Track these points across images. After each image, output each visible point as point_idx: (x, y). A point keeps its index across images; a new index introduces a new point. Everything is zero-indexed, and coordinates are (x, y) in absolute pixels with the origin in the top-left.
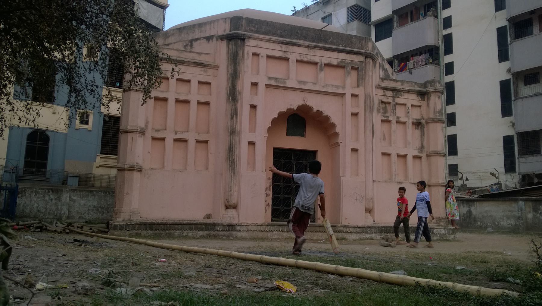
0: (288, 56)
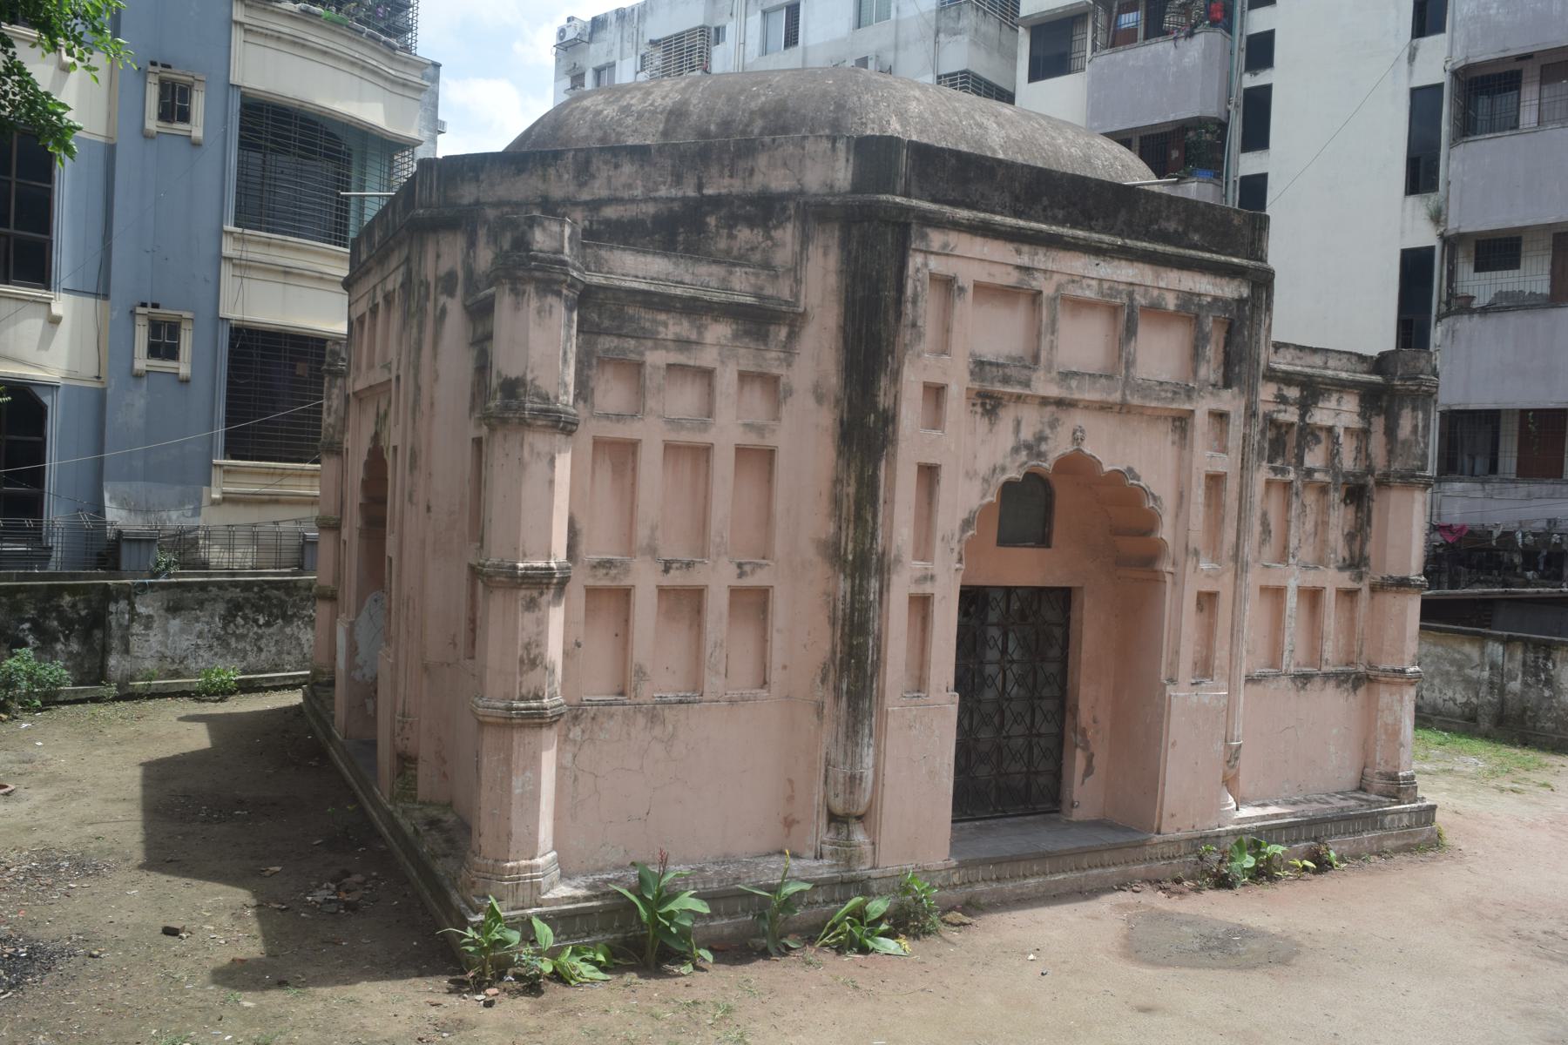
0: (1038, 282)
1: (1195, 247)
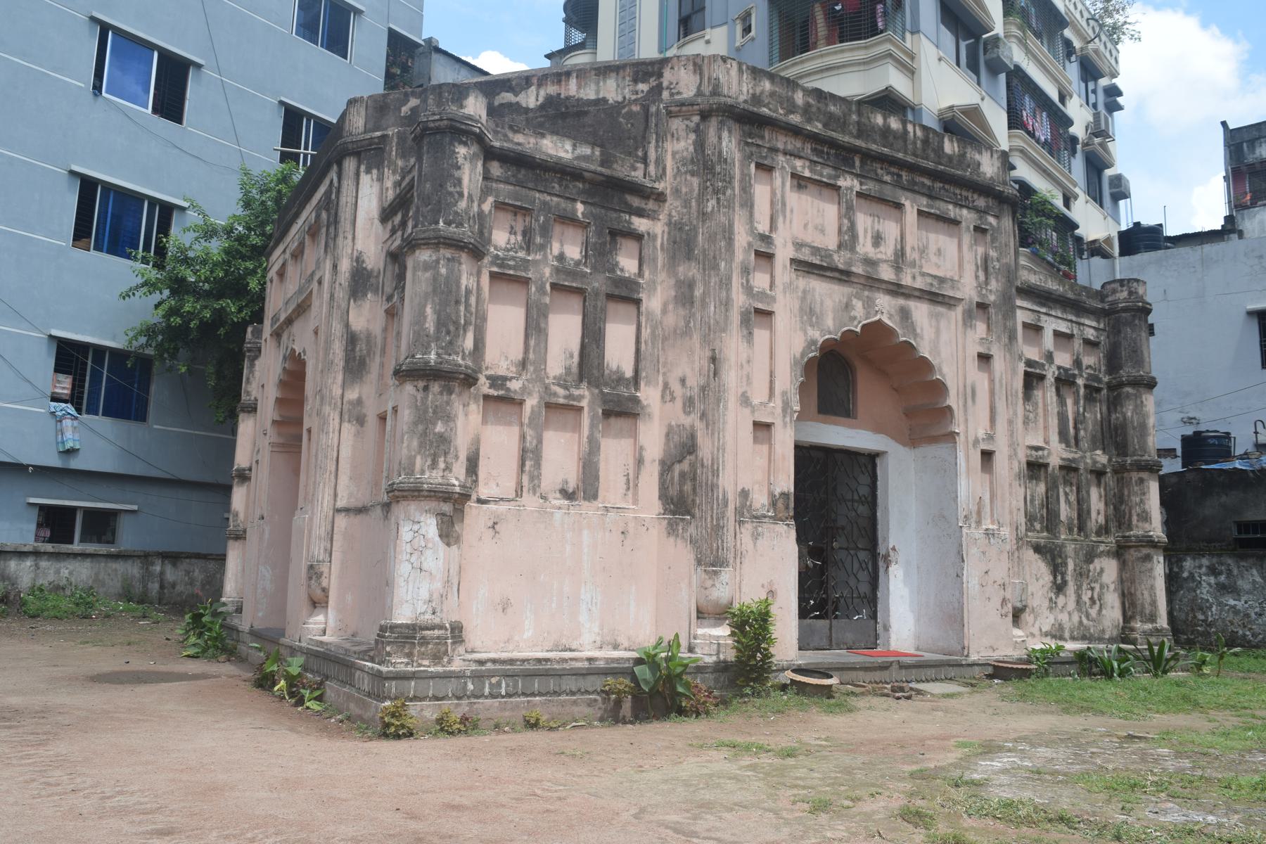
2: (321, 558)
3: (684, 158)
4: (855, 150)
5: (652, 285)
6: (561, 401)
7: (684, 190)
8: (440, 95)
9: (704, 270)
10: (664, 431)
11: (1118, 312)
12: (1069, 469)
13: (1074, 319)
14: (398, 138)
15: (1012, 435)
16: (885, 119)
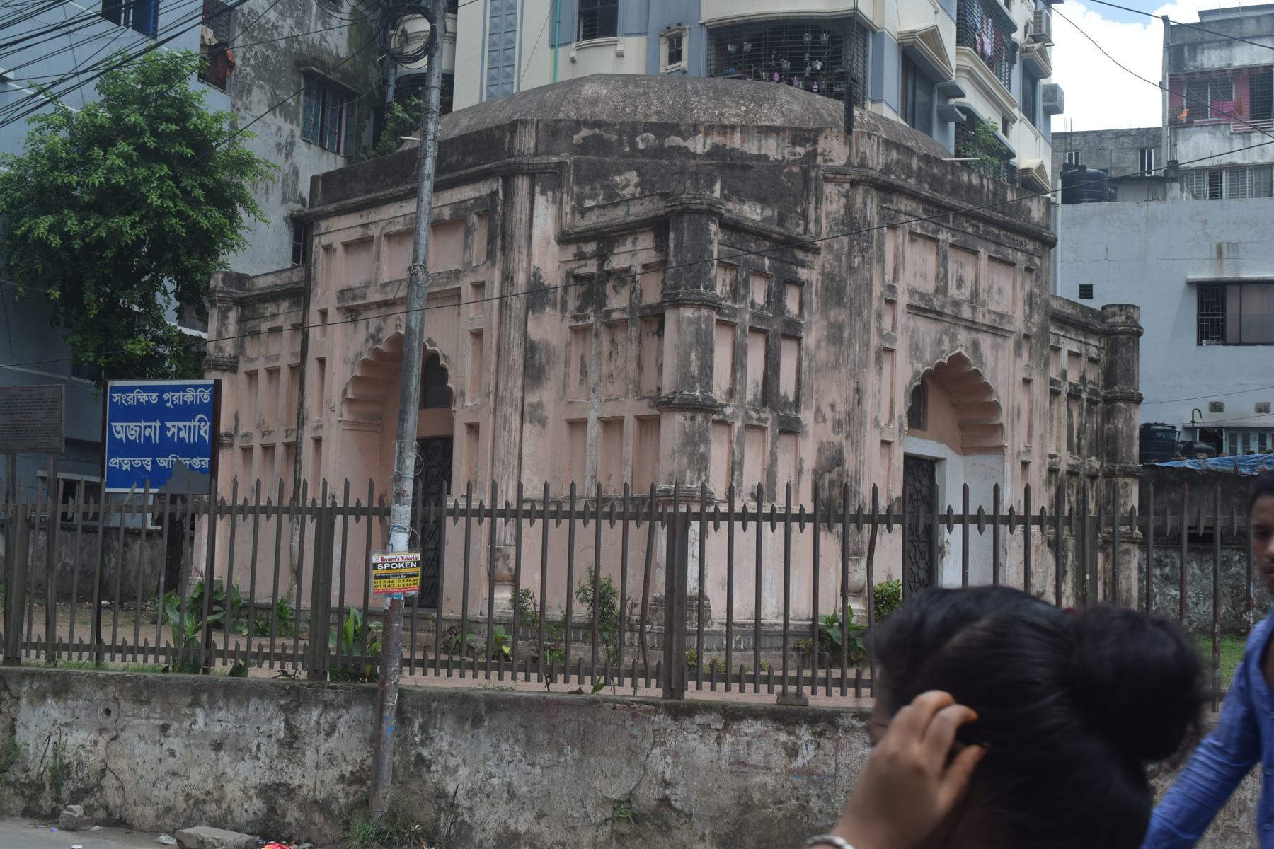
1: (471, 166)
2: (508, 542)
3: (835, 220)
4: (950, 209)
5: (810, 322)
6: (755, 423)
7: (836, 246)
8: (697, 181)
9: (851, 315)
10: (817, 446)
11: (1116, 334)
12: (1072, 473)
13: (1083, 340)
14: (575, 165)
15: (1042, 448)
16: (969, 177)
